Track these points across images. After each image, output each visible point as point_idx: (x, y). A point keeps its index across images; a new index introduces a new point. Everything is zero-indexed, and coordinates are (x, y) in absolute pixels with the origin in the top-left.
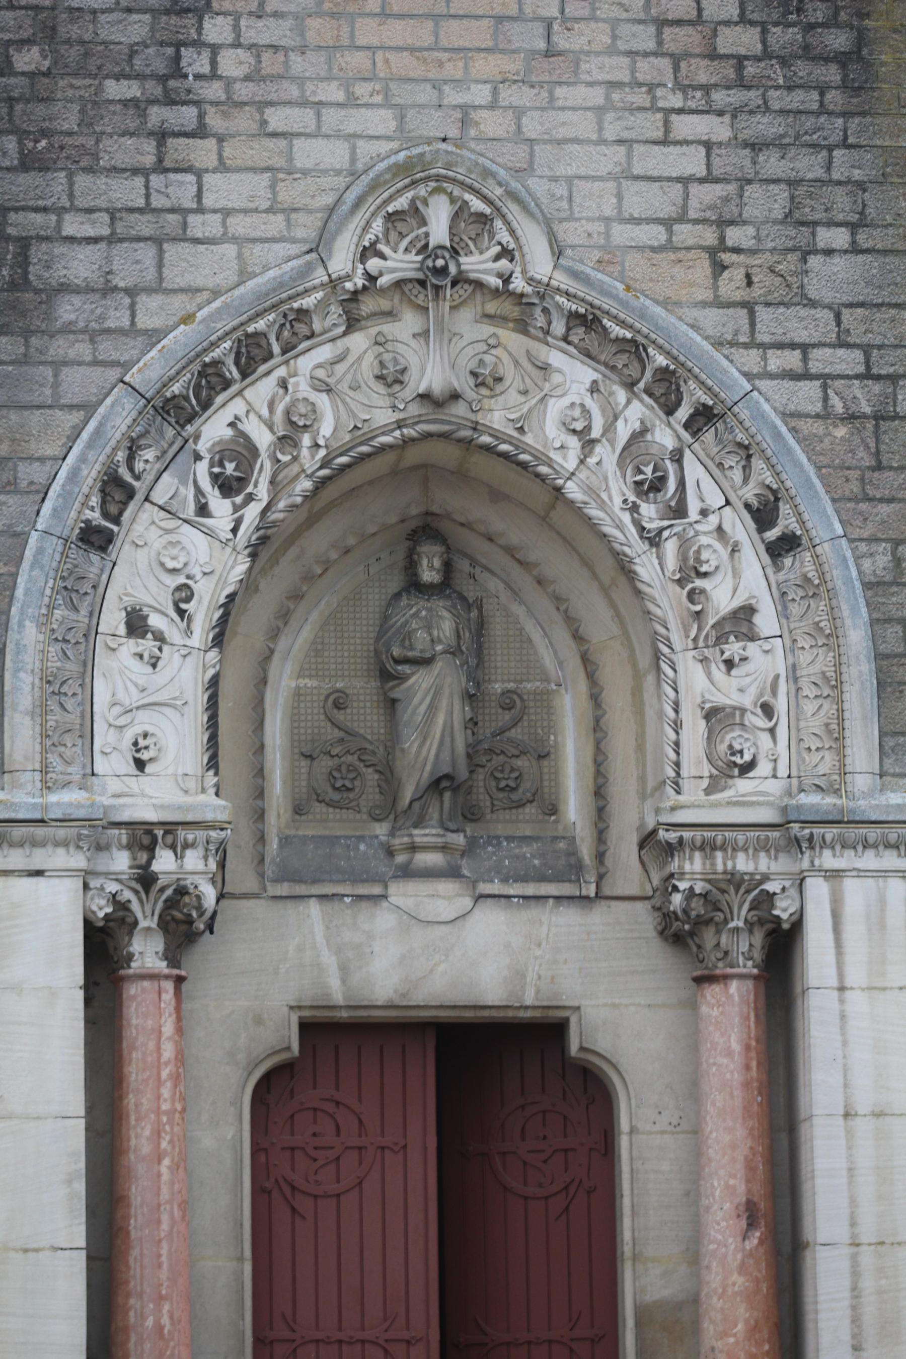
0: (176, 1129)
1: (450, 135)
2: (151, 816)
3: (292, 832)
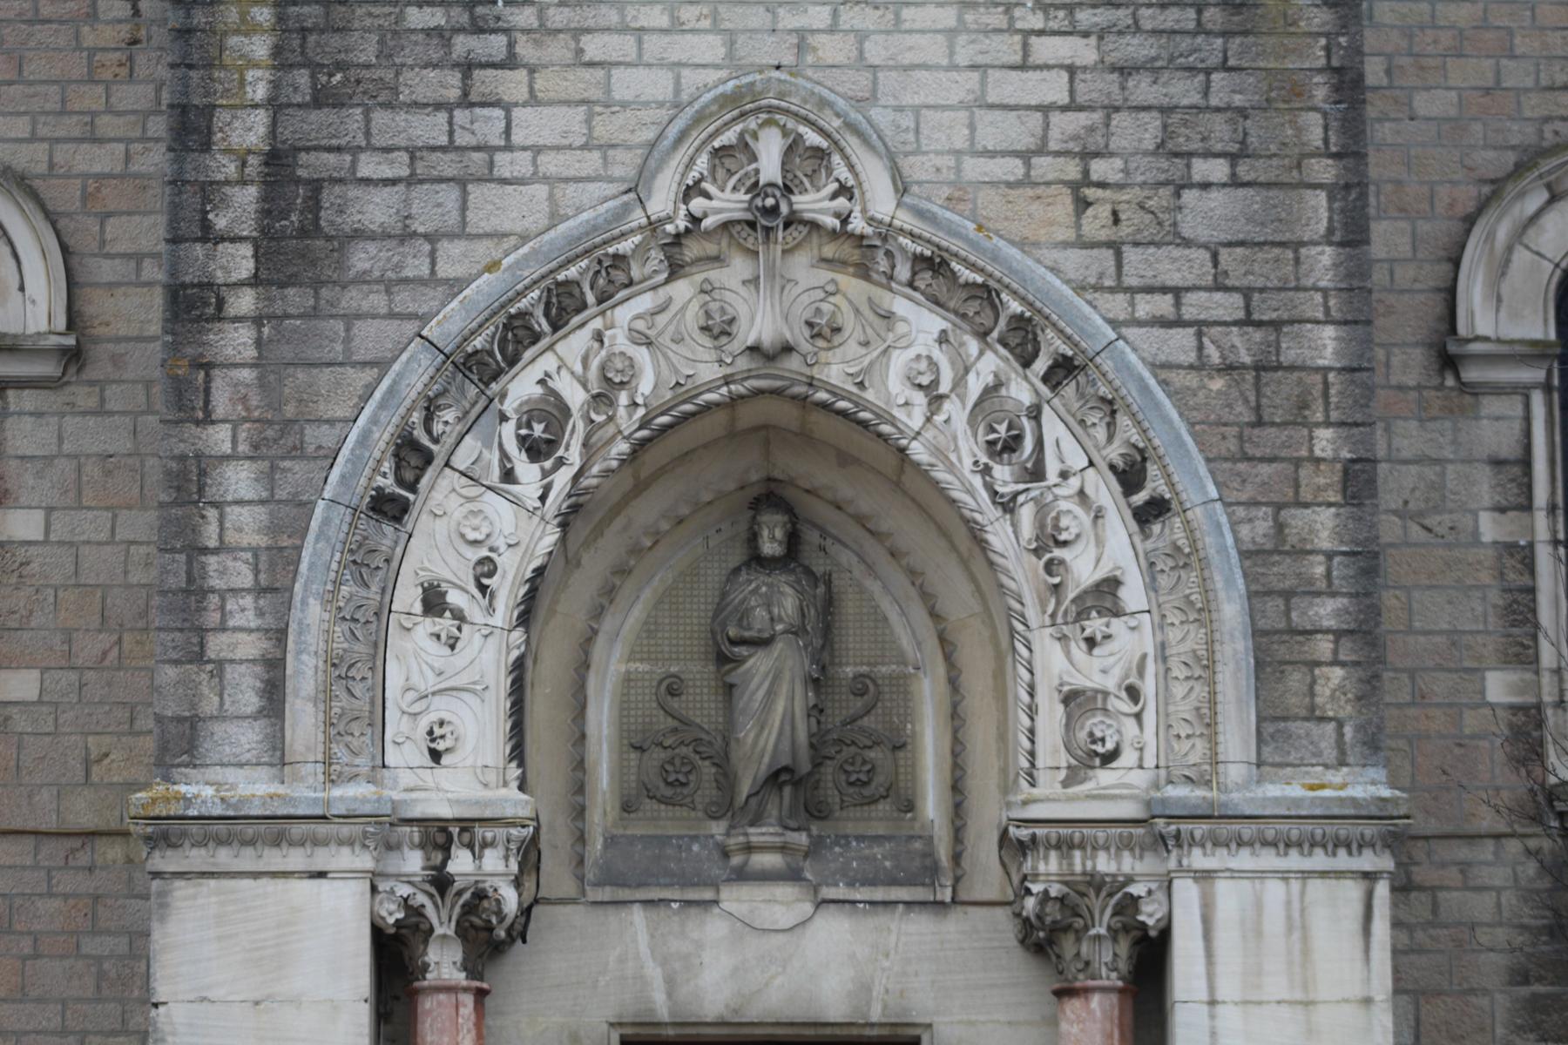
1: (785, 62)
2: (446, 812)
3: (621, 832)
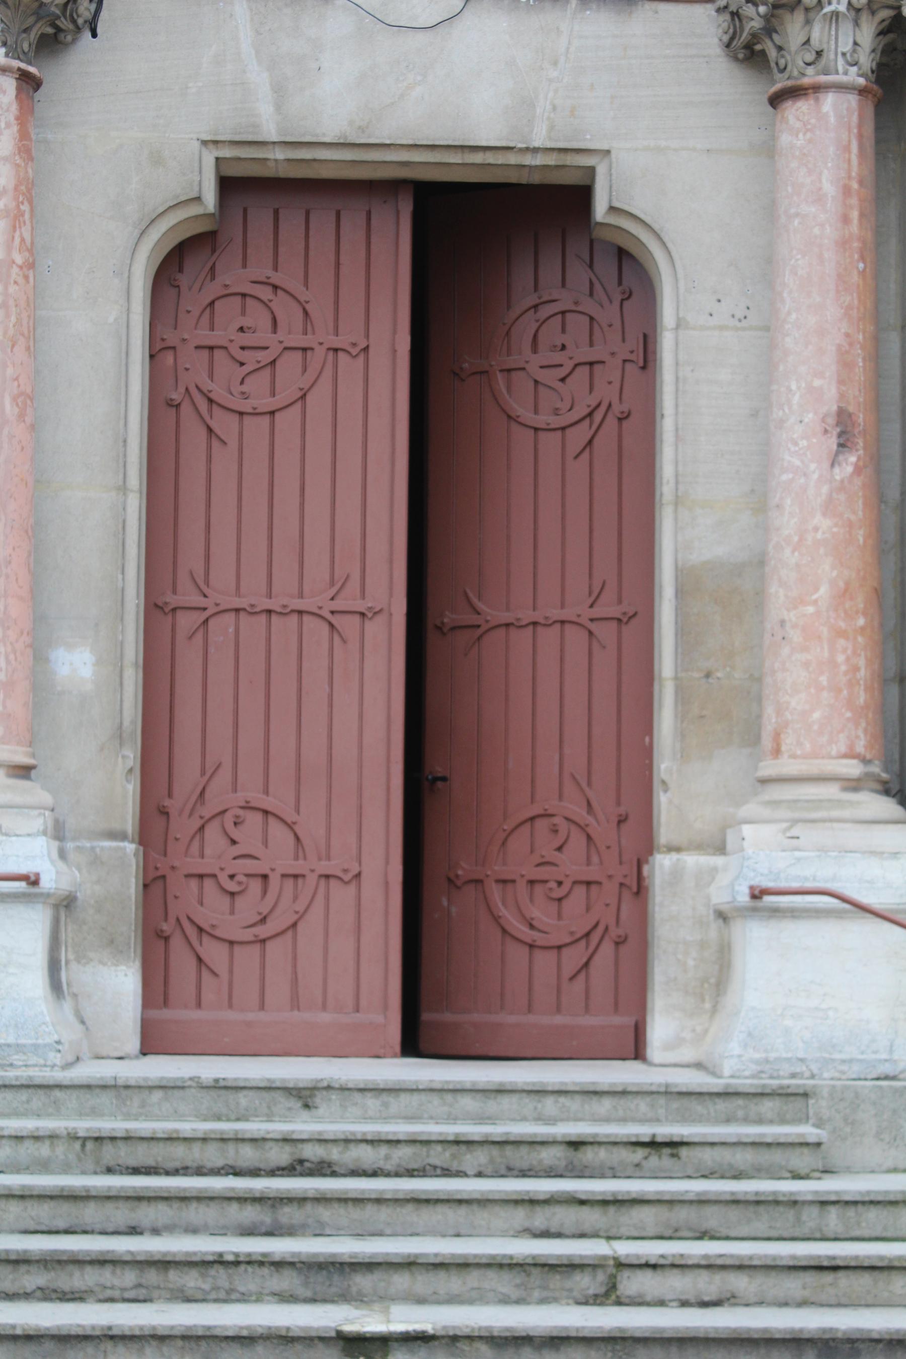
0: (12, 289)
